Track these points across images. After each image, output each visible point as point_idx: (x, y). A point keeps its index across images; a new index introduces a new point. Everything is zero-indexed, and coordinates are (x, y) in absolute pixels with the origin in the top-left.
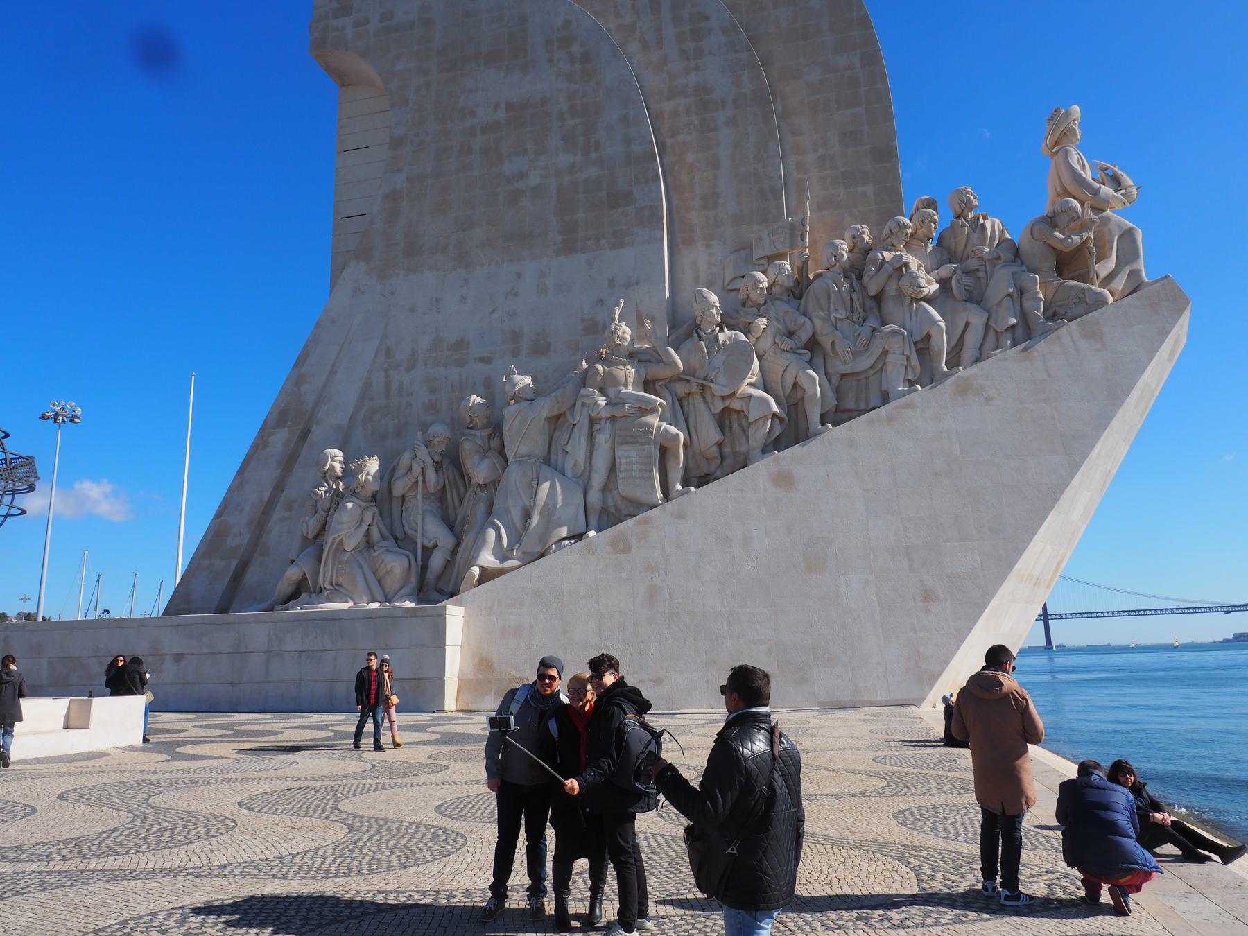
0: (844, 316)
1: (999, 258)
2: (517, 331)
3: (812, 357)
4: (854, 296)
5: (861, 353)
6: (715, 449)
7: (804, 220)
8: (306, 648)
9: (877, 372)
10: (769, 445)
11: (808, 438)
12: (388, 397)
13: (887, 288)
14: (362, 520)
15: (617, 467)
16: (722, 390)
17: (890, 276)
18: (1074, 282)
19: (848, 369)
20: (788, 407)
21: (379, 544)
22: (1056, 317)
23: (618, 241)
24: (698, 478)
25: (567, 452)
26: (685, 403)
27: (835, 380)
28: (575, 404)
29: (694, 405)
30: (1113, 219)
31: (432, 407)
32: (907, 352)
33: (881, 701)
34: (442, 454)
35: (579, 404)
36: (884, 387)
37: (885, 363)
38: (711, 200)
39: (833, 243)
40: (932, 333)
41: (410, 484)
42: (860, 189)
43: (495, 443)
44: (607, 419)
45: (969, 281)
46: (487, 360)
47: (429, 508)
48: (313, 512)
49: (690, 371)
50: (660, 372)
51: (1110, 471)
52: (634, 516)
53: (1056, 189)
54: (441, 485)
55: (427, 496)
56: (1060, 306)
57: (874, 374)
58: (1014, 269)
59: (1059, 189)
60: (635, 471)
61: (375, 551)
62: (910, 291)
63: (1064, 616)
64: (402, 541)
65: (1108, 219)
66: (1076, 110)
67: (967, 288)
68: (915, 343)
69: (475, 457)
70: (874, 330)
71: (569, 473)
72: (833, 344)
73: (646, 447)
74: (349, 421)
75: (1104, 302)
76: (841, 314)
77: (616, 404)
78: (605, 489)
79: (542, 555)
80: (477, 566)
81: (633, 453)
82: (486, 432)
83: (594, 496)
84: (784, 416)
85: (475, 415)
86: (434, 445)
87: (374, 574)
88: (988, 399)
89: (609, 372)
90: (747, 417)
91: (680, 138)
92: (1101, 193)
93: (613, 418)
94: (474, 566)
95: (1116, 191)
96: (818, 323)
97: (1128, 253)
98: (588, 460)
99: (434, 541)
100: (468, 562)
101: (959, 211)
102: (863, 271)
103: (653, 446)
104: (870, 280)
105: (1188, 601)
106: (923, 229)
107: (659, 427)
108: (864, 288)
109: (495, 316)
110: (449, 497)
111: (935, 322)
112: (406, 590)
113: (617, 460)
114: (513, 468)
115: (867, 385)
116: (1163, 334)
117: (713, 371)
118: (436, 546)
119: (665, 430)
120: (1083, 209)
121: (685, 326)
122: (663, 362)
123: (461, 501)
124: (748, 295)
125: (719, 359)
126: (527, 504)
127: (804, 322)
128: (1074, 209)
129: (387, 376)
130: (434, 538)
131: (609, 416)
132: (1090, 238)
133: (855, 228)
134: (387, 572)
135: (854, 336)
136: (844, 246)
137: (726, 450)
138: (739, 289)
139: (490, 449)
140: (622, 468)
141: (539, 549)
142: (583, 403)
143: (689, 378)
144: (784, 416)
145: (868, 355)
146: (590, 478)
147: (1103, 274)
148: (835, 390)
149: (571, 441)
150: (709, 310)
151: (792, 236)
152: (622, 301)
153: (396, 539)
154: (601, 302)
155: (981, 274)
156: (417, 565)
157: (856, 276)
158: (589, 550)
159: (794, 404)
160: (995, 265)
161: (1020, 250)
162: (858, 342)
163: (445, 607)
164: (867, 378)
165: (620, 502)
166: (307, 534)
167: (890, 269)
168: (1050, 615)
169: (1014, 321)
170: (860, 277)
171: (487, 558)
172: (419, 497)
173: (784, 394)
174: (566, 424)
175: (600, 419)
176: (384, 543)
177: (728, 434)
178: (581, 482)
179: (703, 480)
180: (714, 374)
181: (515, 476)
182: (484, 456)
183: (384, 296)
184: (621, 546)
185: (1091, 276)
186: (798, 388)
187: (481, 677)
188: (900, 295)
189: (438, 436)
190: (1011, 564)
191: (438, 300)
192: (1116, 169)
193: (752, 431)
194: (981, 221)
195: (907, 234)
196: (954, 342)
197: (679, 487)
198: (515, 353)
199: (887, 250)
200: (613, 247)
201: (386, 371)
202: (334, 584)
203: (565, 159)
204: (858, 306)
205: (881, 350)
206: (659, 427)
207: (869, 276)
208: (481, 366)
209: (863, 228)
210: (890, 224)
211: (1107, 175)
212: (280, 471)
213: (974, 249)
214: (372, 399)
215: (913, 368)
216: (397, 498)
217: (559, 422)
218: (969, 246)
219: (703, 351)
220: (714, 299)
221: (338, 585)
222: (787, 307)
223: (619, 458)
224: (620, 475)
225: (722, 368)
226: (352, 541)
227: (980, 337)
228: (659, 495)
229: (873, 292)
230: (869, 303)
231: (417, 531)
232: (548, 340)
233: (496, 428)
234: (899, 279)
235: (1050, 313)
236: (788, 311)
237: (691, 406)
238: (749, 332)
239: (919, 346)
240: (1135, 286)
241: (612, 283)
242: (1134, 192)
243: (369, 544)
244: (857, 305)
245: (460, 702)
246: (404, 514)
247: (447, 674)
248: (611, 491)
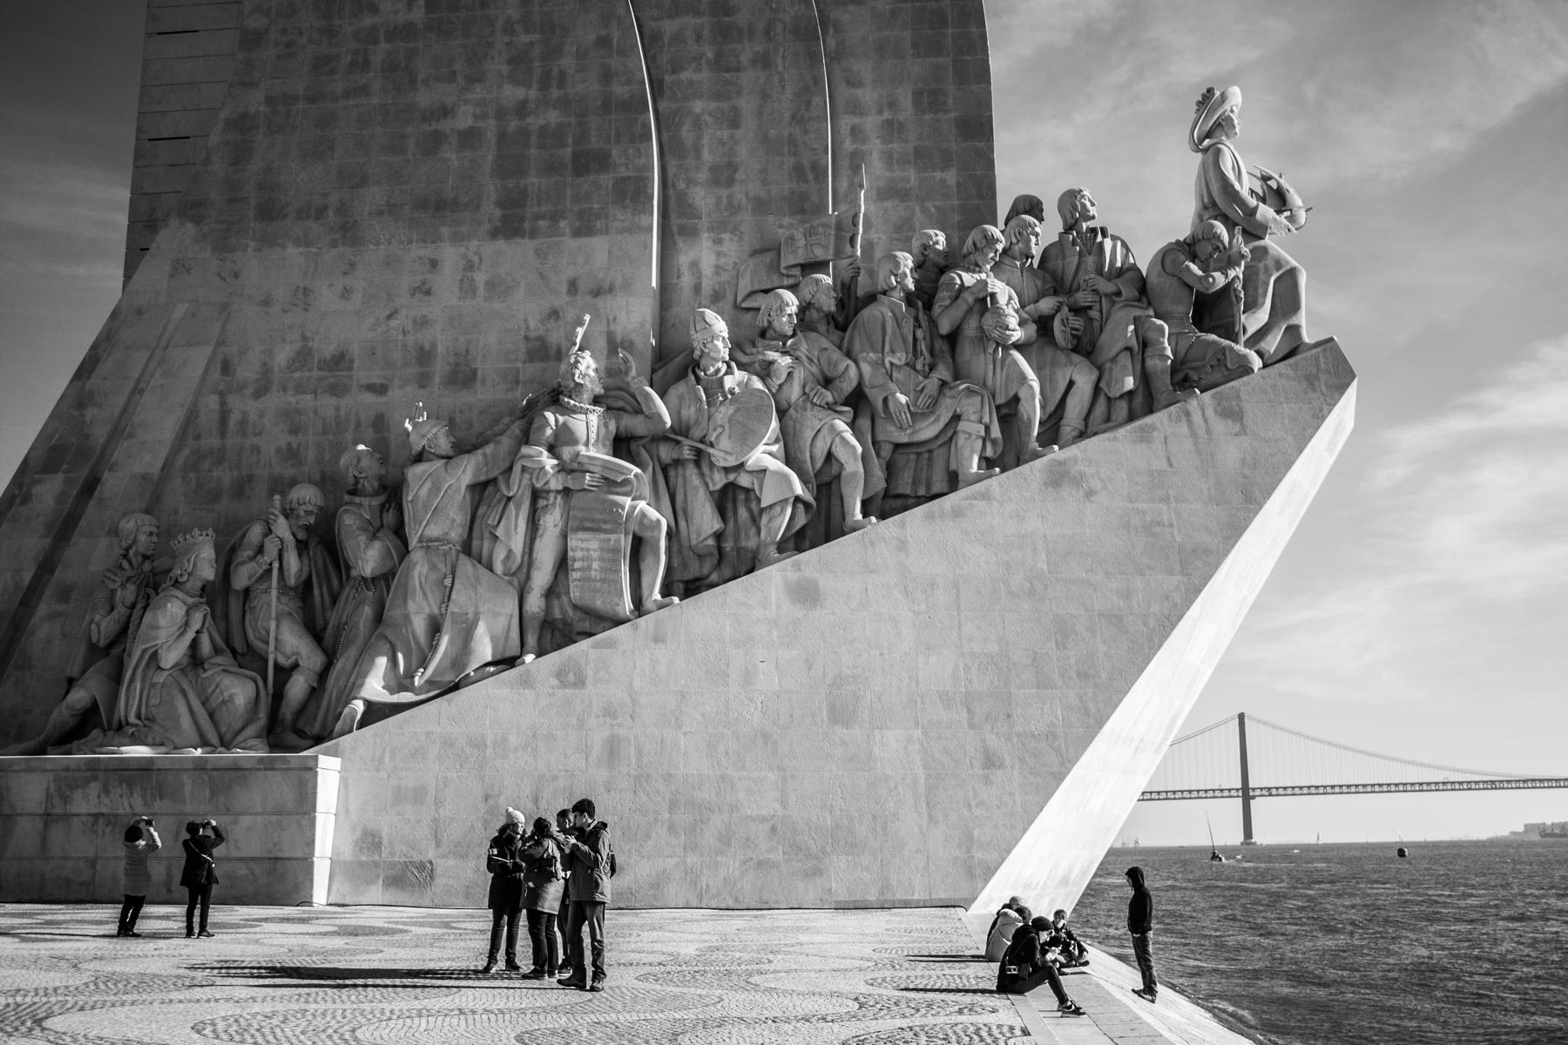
0: (903, 362)
1: (1119, 294)
2: (427, 347)
4: (920, 334)
5: (924, 415)
6: (711, 542)
7: (856, 216)
8: (104, 810)
9: (944, 443)
10: (790, 538)
11: (843, 534)
12: (223, 435)
13: (965, 326)
14: (187, 624)
15: (570, 563)
16: (725, 459)
17: (970, 310)
18: (1213, 337)
19: (904, 439)
20: (818, 486)
21: (212, 661)
22: (1187, 384)
23: (585, 229)
24: (685, 585)
25: (497, 537)
26: (672, 473)
27: (886, 451)
28: (510, 469)
29: (684, 476)
30: (1271, 251)
31: (292, 455)
32: (986, 419)
33: (919, 901)
34: (307, 528)
35: (517, 468)
36: (953, 467)
37: (955, 433)
38: (724, 174)
39: (895, 256)
40: (1022, 394)
41: (261, 571)
42: (938, 175)
43: (390, 517)
44: (558, 492)
45: (1077, 322)
46: (380, 389)
47: (287, 609)
48: (108, 606)
49: (681, 430)
50: (636, 425)
51: (1245, 598)
52: (591, 635)
53: (1203, 201)
54: (303, 578)
55: (283, 587)
56: (1194, 369)
57: (940, 446)
58: (1138, 312)
59: (1206, 200)
60: (596, 570)
61: (205, 671)
62: (996, 334)
63: (1274, 792)
64: (248, 657)
65: (1265, 250)
66: (1236, 96)
67: (1074, 332)
68: (998, 408)
69: (360, 538)
70: (944, 384)
71: (499, 568)
72: (885, 400)
73: (613, 537)
74: (162, 470)
75: (1246, 370)
76: (900, 358)
77: (572, 471)
78: (550, 593)
79: (456, 687)
80: (360, 699)
81: (594, 545)
82: (376, 502)
83: (535, 603)
84: (809, 498)
85: (363, 475)
86: (298, 516)
87: (203, 704)
88: (1090, 494)
89: (565, 424)
90: (759, 500)
91: (685, 76)
92: (1258, 216)
93: (566, 492)
94: (355, 698)
95: (1279, 212)
96: (866, 369)
97: (1287, 301)
98: (527, 551)
99: (294, 657)
100: (347, 692)
101: (1071, 221)
102: (934, 297)
103: (623, 536)
104: (943, 311)
105: (1462, 771)
106: (1020, 245)
107: (633, 508)
108: (933, 323)
109: (393, 323)
110: (316, 592)
111: (1023, 378)
112: (251, 730)
113: (570, 554)
114: (417, 556)
115: (930, 459)
116: (1319, 418)
117: (715, 430)
118: (296, 666)
119: (643, 515)
120: (1231, 237)
121: (681, 356)
122: (641, 412)
123: (335, 599)
124: (769, 322)
125: (723, 414)
126: (436, 611)
127: (848, 366)
128: (1218, 237)
129: (223, 404)
130: (293, 655)
131: (560, 488)
132: (1238, 278)
133: (927, 234)
134: (223, 702)
135: (915, 390)
136: (907, 261)
137: (726, 545)
138: (759, 309)
139: (382, 526)
140: (577, 565)
141: (449, 677)
142: (523, 467)
143: (679, 438)
144: (809, 498)
145: (932, 419)
146: (528, 577)
147: (1251, 330)
148: (885, 467)
149: (502, 523)
150: (712, 341)
151: (838, 238)
152: (587, 318)
153: (234, 652)
154: (555, 314)
155: (1094, 314)
156: (267, 694)
157: (923, 304)
158: (526, 682)
160: (1113, 303)
161: (1148, 286)
162: (920, 400)
163: (316, 758)
164: (930, 452)
165: (571, 614)
166: (99, 640)
167: (970, 299)
168: (1253, 789)
169: (1129, 383)
170: (928, 306)
171: (375, 686)
172: (274, 593)
173: (813, 468)
174: (498, 496)
175: (548, 492)
176: (218, 660)
177: (731, 524)
178: (516, 582)
179: (691, 588)
180: (715, 434)
181: (419, 568)
182: (374, 537)
183: (224, 280)
184: (571, 677)
185: (1236, 330)
186: (833, 460)
187: (364, 858)
188: (983, 338)
189: (305, 503)
190: (1101, 723)
191: (306, 291)
192: (1282, 181)
193: (765, 519)
194: (1099, 238)
195: (997, 250)
196: (1051, 408)
197: (657, 596)
198: (423, 381)
199: (968, 270)
200: (577, 233)
201: (222, 394)
202: (143, 717)
203: (511, 94)
204: (923, 348)
205: (951, 415)
206: (633, 508)
207: (940, 306)
208: (369, 398)
209: (937, 235)
210: (974, 235)
211: (1270, 187)
212: (49, 540)
213: (1087, 277)
214: (198, 437)
215: (994, 442)
216: (237, 592)
217: (487, 493)
218: (1081, 273)
219: (701, 401)
220: (720, 326)
221: (147, 719)
222: (825, 343)
223: (572, 550)
224: (575, 575)
225: (727, 426)
226: (173, 655)
227: (1086, 405)
228: (628, 604)
229: (945, 327)
230: (940, 345)
231: (268, 643)
232: (474, 366)
233: (392, 493)
234: (982, 315)
235: (1180, 376)
236: (826, 349)
237: (680, 479)
238: (769, 375)
239: (1004, 411)
240: (1293, 348)
241: (573, 286)
242: (1302, 216)
243: (195, 659)
244: (923, 346)
245: (333, 893)
246: (248, 617)
247: (317, 853)
248: (558, 597)
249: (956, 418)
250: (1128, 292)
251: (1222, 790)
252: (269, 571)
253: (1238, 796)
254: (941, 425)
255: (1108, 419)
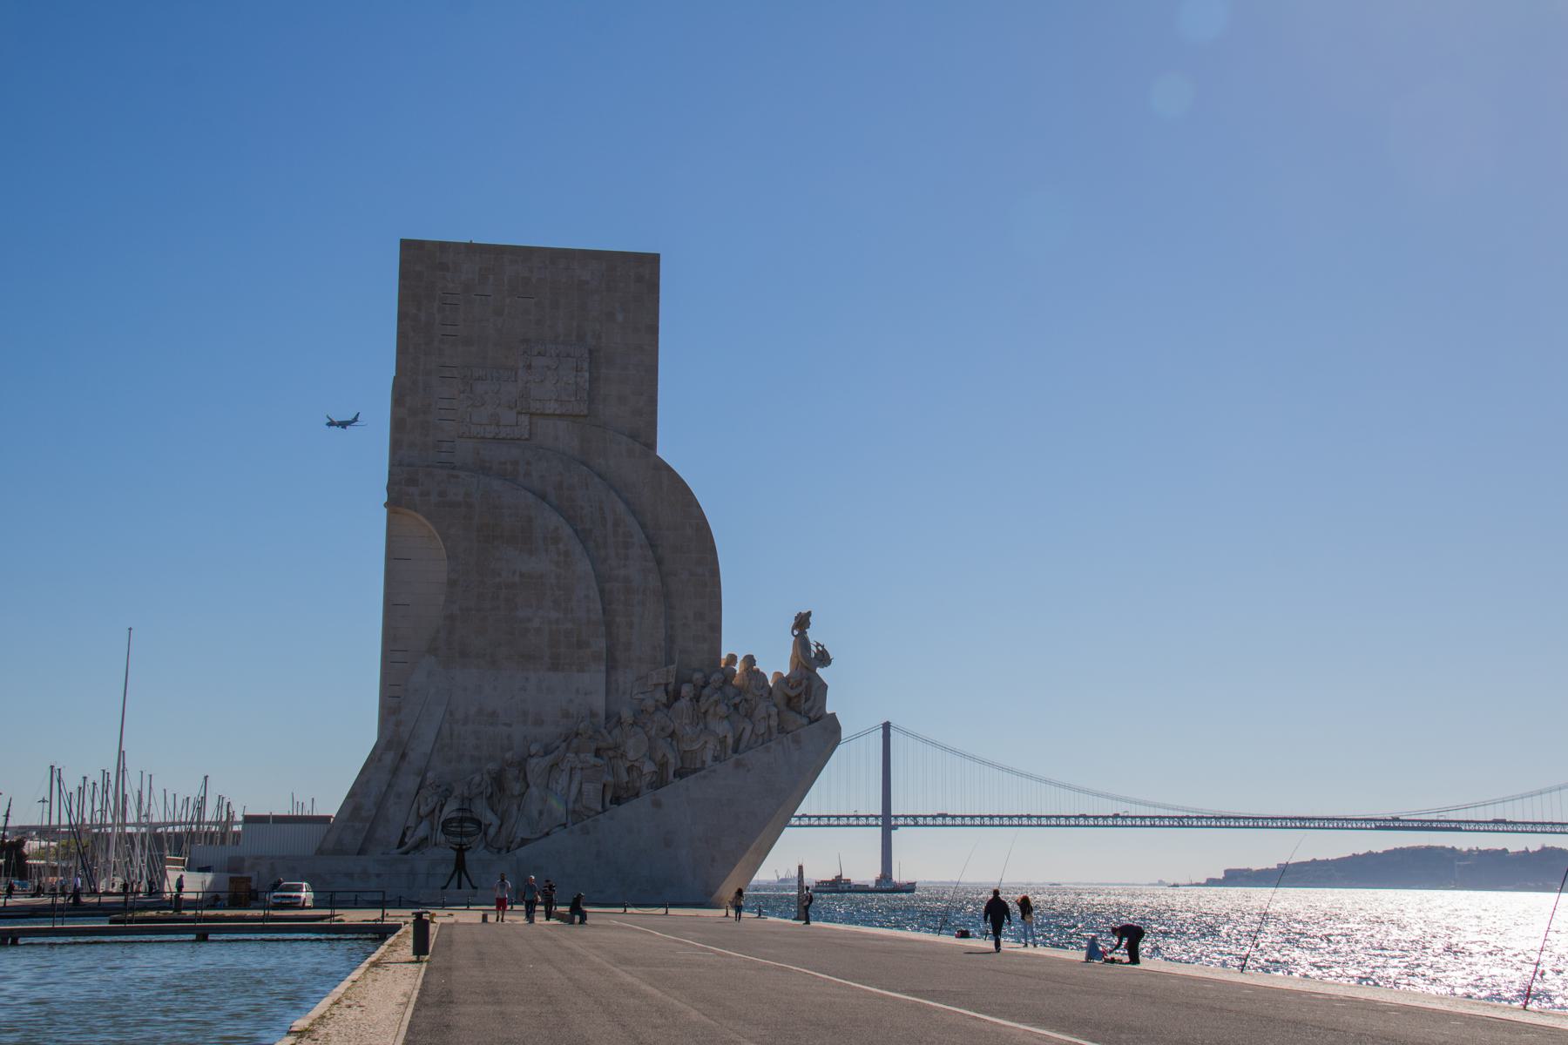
1: (762, 695)
3: (672, 740)
6: (625, 785)
43: (522, 775)
46: (510, 725)
49: (616, 747)
63: (921, 821)
70: (701, 729)
76: (687, 721)
78: (576, 801)
83: (570, 806)
88: (749, 770)
93: (582, 769)
118: (490, 825)
155: (753, 702)
159: (663, 766)
168: (896, 817)
170: (698, 701)
181: (534, 790)
229: (703, 711)
235: (780, 727)
249: (706, 742)
250: (766, 695)
251: (858, 817)
252: (482, 793)
253: (877, 825)
254: (699, 745)
255: (756, 742)
